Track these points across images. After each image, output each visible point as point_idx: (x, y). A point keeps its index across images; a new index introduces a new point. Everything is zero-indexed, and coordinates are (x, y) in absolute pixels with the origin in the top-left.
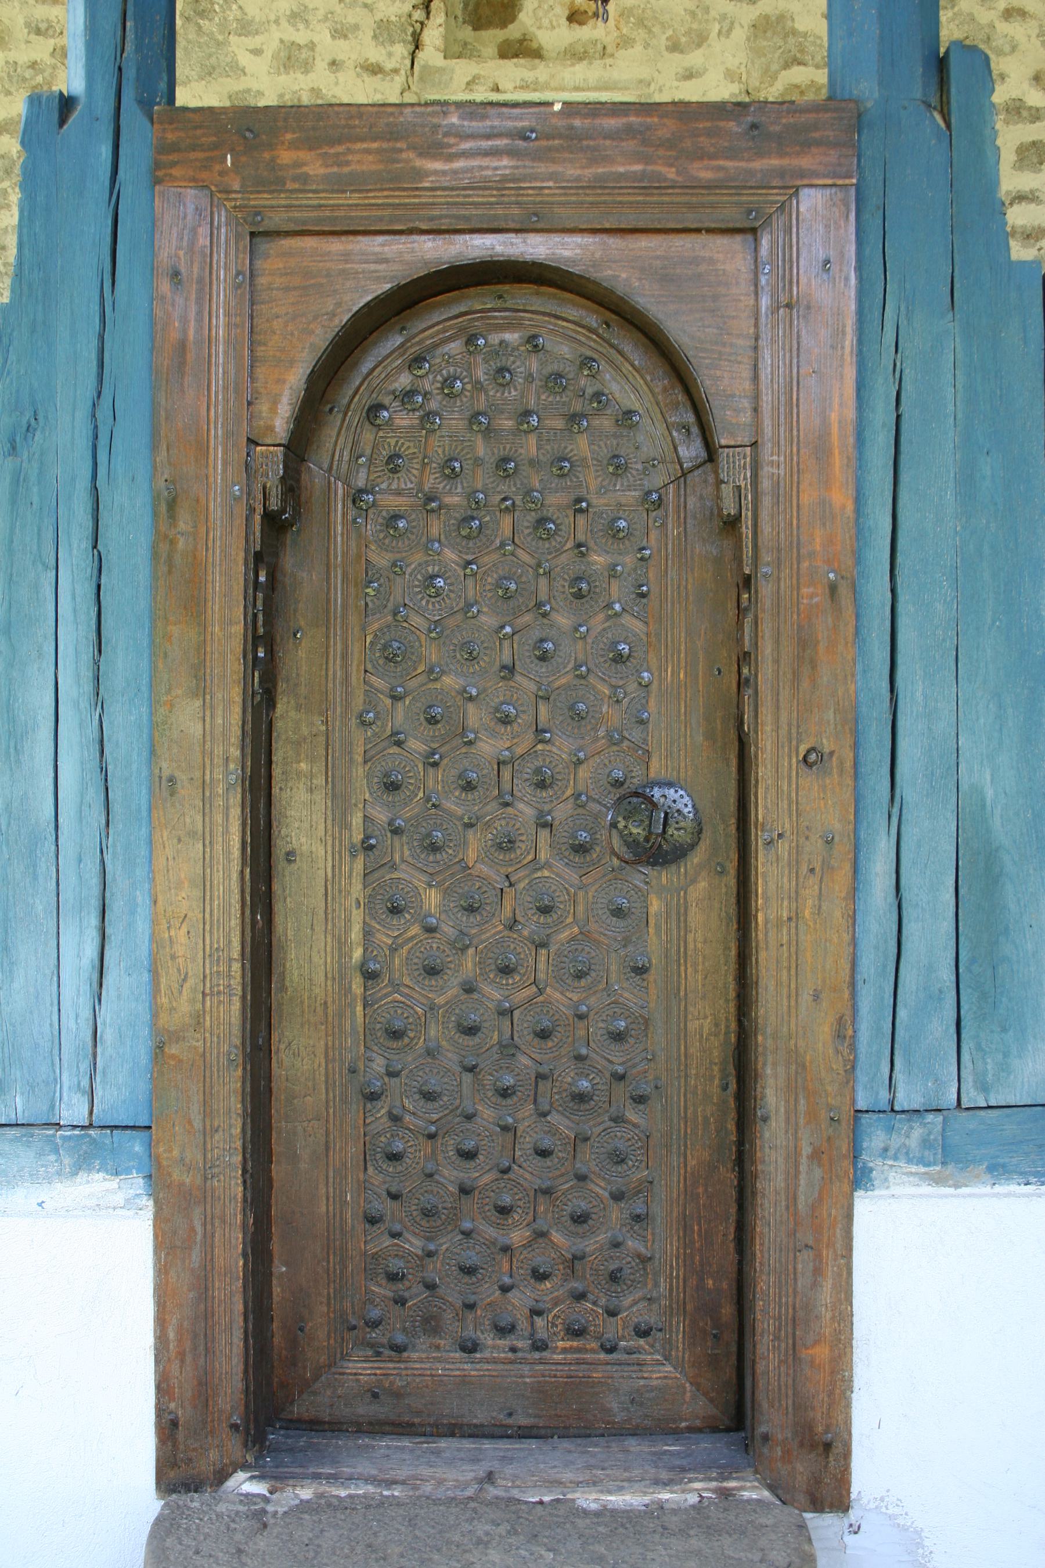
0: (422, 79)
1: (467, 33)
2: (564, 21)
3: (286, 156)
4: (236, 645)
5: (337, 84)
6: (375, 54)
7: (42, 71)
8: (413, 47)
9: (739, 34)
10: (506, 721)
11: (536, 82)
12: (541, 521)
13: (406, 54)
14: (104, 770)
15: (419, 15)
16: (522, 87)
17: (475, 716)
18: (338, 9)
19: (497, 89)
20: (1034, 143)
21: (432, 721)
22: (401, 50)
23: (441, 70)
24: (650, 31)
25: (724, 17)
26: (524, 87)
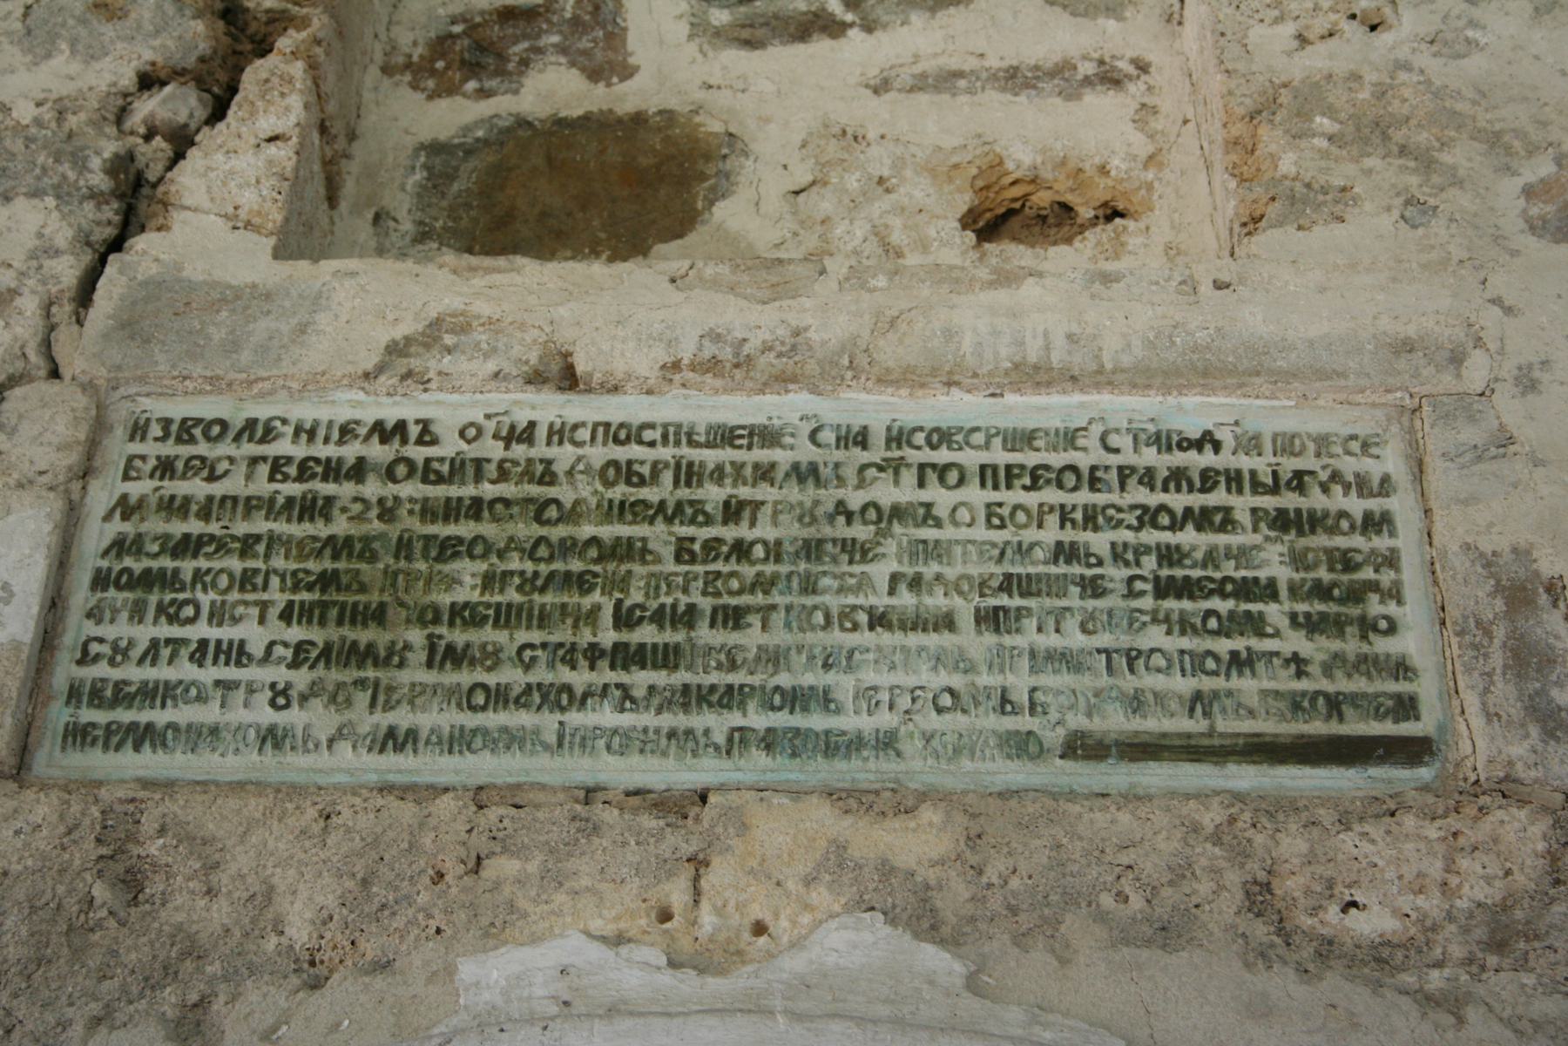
0: (129, 326)
13: (62, 235)
16: (712, 366)
24: (1426, 163)
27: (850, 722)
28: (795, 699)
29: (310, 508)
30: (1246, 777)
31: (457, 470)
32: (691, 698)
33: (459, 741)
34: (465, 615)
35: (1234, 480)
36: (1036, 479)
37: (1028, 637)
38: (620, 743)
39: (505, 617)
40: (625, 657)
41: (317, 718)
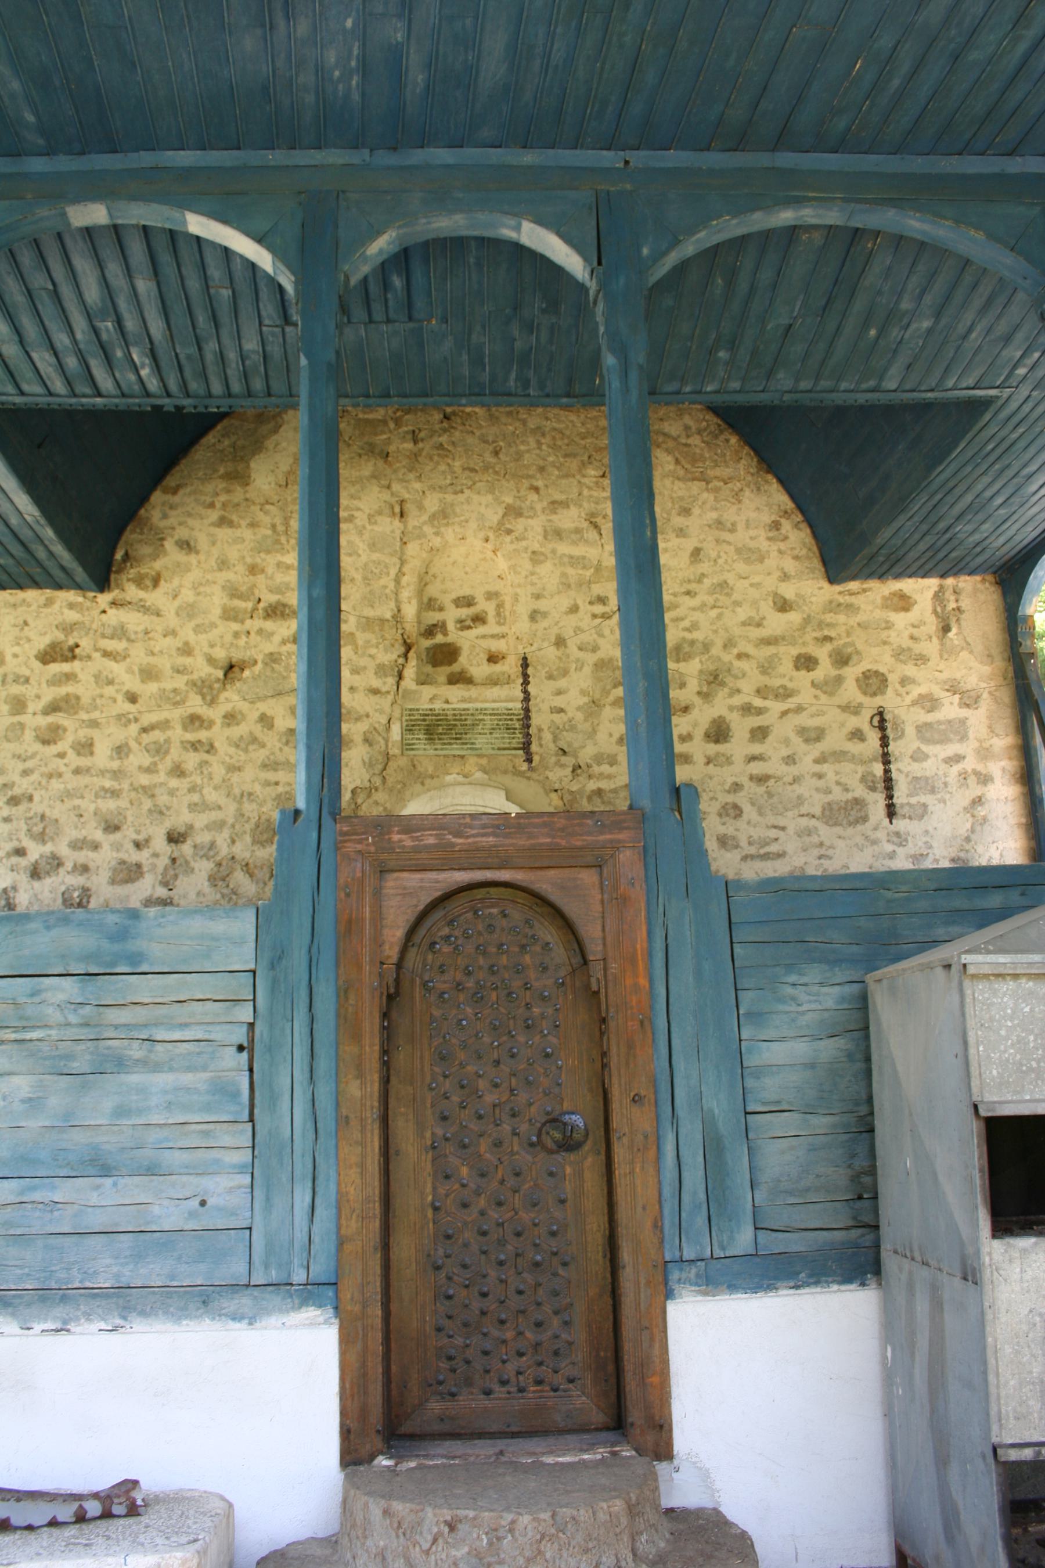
0: (403, 697)
1: (429, 669)
2: (485, 662)
3: (396, 837)
4: (376, 1055)
5: (354, 700)
6: (376, 683)
7: (180, 694)
8: (397, 679)
9: (587, 670)
10: (496, 1086)
11: (470, 698)
12: (510, 994)
14: (314, 1113)
15: (401, 661)
17: (482, 1084)
18: (354, 658)
19: (447, 702)
20: (759, 727)
21: (462, 1087)
22: (391, 681)
23: (415, 692)
25: (578, 660)
26: (463, 701)
27: (477, 746)
28: (473, 744)
29: (424, 720)
30: (513, 752)
31: (439, 715)
32: (463, 744)
33: (442, 749)
34: (441, 734)
35: (513, 714)
36: (495, 715)
37: (494, 735)
38: (457, 749)
39: (445, 734)
40: (457, 739)
41: (427, 747)
